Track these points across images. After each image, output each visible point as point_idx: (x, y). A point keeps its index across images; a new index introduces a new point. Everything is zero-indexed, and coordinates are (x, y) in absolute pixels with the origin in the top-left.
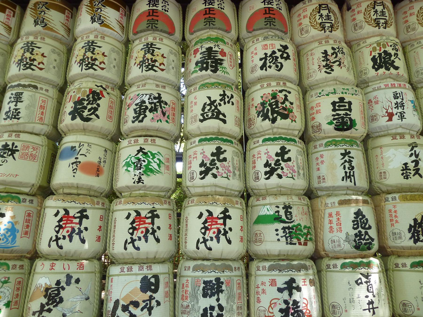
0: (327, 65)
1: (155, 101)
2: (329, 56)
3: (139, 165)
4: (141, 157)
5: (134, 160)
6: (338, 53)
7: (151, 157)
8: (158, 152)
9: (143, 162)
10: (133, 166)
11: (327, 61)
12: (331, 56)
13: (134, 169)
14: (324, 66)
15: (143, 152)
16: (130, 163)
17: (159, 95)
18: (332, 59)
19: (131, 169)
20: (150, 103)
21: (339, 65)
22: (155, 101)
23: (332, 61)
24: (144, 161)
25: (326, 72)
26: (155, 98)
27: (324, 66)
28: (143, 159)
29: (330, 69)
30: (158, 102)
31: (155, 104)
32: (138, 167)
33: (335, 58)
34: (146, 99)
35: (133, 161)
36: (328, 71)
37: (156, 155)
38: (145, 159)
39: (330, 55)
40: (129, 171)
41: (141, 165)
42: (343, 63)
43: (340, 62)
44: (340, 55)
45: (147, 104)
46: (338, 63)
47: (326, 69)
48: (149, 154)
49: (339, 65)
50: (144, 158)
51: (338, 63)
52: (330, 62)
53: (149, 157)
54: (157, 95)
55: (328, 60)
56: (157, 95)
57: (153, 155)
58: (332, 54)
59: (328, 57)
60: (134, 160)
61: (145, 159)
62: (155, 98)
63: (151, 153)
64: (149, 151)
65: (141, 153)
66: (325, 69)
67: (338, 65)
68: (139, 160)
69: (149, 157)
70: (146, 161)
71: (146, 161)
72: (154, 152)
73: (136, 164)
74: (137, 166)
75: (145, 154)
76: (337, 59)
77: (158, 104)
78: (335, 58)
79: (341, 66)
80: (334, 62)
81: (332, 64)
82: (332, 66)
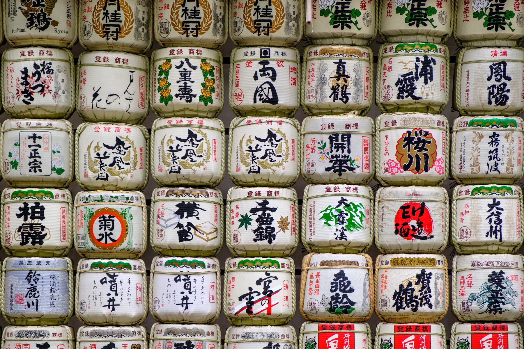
0: (25, 92)
2: (30, 77)
3: (341, 219)
4: (343, 210)
5: (335, 213)
6: (42, 73)
7: (354, 210)
8: (360, 204)
9: (345, 216)
10: (334, 220)
11: (26, 85)
12: (32, 78)
13: (336, 223)
14: (22, 92)
15: (345, 204)
16: (331, 215)
18: (33, 82)
19: (332, 223)
21: (42, 91)
23: (32, 86)
24: (347, 214)
25: (24, 101)
27: (22, 92)
28: (345, 212)
29: (29, 98)
32: (340, 221)
33: (36, 81)
35: (335, 214)
36: (26, 99)
37: (358, 208)
38: (347, 212)
39: (31, 76)
40: (330, 225)
41: (343, 218)
42: (48, 88)
43: (43, 87)
44: (44, 76)
46: (40, 88)
47: (25, 96)
48: (352, 206)
49: (42, 91)
50: (346, 210)
51: (40, 88)
53: (352, 210)
55: (27, 83)
57: (355, 207)
58: (34, 75)
59: (28, 78)
60: (335, 213)
61: (347, 212)
63: (353, 204)
64: (351, 203)
65: (343, 205)
66: (22, 97)
67: (39, 92)
68: (341, 213)
69: (352, 210)
70: (349, 214)
71: (349, 214)
72: (356, 204)
73: (337, 217)
74: (339, 219)
75: (348, 206)
76: (39, 82)
78: (36, 81)
79: (45, 92)
80: (35, 88)
81: (32, 90)
82: (31, 93)
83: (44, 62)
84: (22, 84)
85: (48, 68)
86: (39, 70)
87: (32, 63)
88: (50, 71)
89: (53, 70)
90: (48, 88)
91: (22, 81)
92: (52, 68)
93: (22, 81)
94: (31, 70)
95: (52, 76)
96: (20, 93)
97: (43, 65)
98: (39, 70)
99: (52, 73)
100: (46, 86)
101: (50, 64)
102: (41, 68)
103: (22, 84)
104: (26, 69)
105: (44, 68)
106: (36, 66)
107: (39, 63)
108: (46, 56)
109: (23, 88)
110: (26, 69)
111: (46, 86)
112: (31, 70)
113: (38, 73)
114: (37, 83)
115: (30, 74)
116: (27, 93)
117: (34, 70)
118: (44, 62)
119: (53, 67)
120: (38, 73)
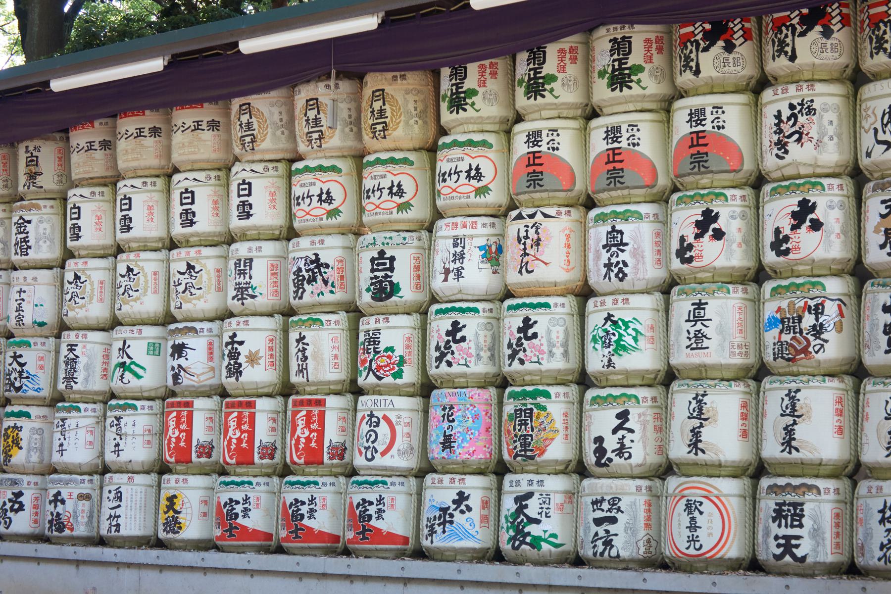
1: (312, 266)
6: (799, 116)
14: (776, 144)
17: (316, 255)
18: (787, 129)
20: (307, 271)
21: (799, 140)
22: (312, 266)
23: (787, 134)
25: (777, 156)
26: (312, 262)
27: (776, 144)
30: (316, 267)
31: (312, 270)
33: (792, 126)
34: (301, 264)
36: (780, 153)
42: (807, 134)
43: (801, 134)
44: (802, 119)
45: (304, 273)
46: (796, 136)
49: (799, 140)
51: (796, 136)
52: (784, 136)
54: (313, 258)
56: (313, 258)
58: (789, 119)
62: (312, 262)
66: (775, 151)
76: (796, 128)
77: (316, 270)
78: (792, 126)
81: (786, 140)
82: (786, 144)
83: (803, 101)
84: (775, 132)
85: (809, 107)
86: (796, 111)
87: (787, 104)
88: (811, 111)
89: (815, 110)
90: (807, 134)
91: (775, 128)
92: (814, 107)
93: (775, 128)
94: (786, 113)
95: (814, 117)
96: (773, 144)
97: (801, 104)
98: (796, 111)
99: (814, 114)
100: (805, 132)
101: (812, 101)
102: (799, 108)
103: (775, 132)
104: (779, 112)
105: (801, 109)
106: (792, 107)
107: (795, 102)
108: (805, 91)
109: (775, 138)
110: (779, 112)
111: (805, 132)
112: (786, 113)
113: (794, 116)
114: (793, 129)
115: (784, 118)
116: (781, 145)
117: (789, 113)
118: (803, 101)
119: (815, 105)
120: (794, 116)
